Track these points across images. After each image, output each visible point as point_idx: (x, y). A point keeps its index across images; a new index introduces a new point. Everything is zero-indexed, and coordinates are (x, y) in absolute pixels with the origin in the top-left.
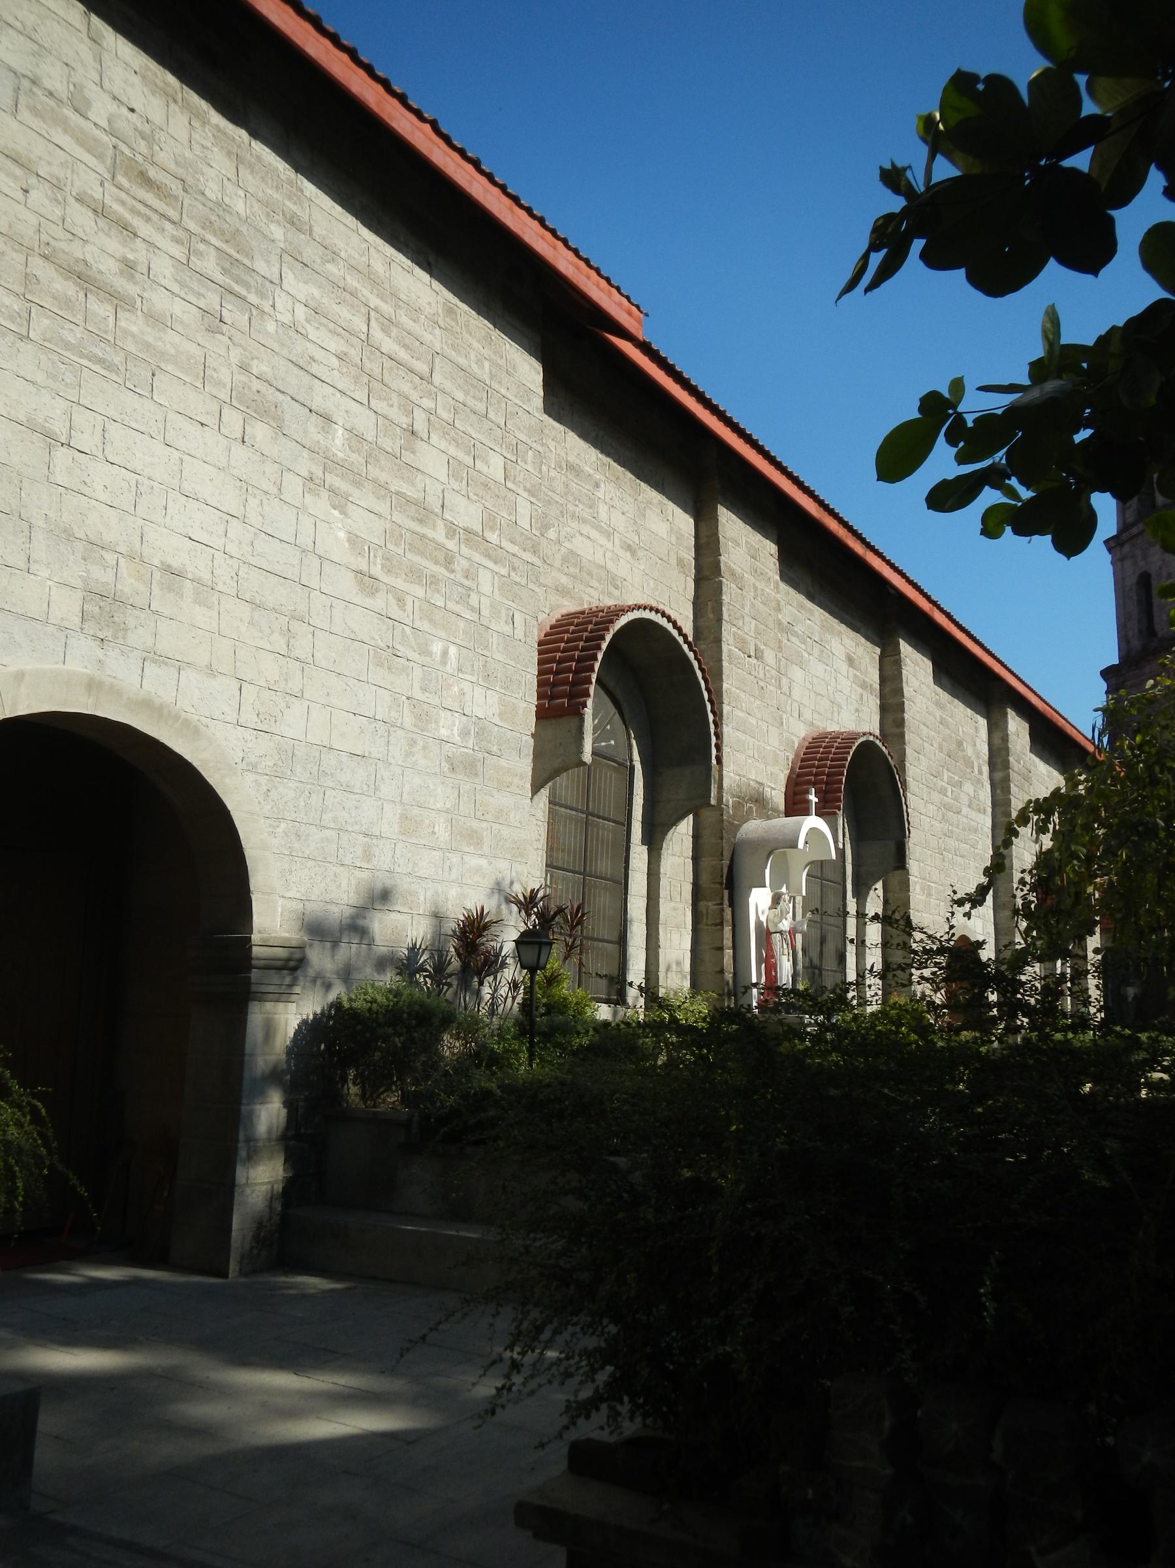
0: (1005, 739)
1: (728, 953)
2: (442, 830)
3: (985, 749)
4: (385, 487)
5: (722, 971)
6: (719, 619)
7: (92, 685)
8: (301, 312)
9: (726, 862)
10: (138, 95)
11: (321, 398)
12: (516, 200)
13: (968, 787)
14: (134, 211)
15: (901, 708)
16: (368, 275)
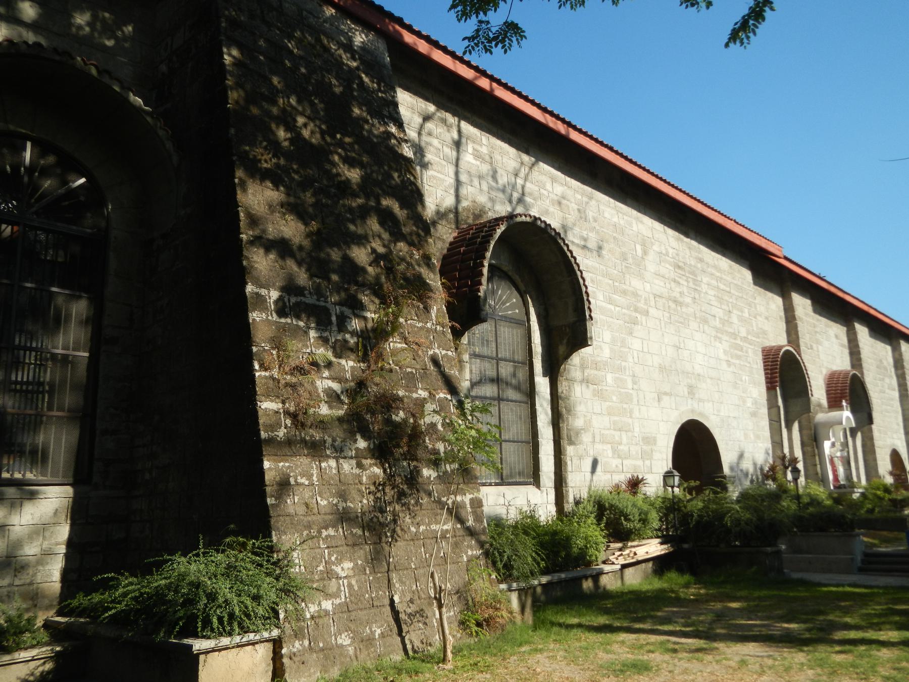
0: (901, 355)
1: (819, 466)
2: (752, 436)
3: (891, 360)
4: (727, 332)
5: (817, 474)
6: (798, 338)
7: (693, 411)
8: (706, 286)
9: (813, 432)
10: (674, 243)
11: (715, 311)
12: (752, 231)
13: (887, 380)
14: (680, 278)
15: (859, 353)
16: (715, 267)
